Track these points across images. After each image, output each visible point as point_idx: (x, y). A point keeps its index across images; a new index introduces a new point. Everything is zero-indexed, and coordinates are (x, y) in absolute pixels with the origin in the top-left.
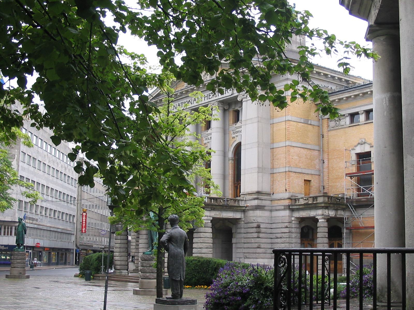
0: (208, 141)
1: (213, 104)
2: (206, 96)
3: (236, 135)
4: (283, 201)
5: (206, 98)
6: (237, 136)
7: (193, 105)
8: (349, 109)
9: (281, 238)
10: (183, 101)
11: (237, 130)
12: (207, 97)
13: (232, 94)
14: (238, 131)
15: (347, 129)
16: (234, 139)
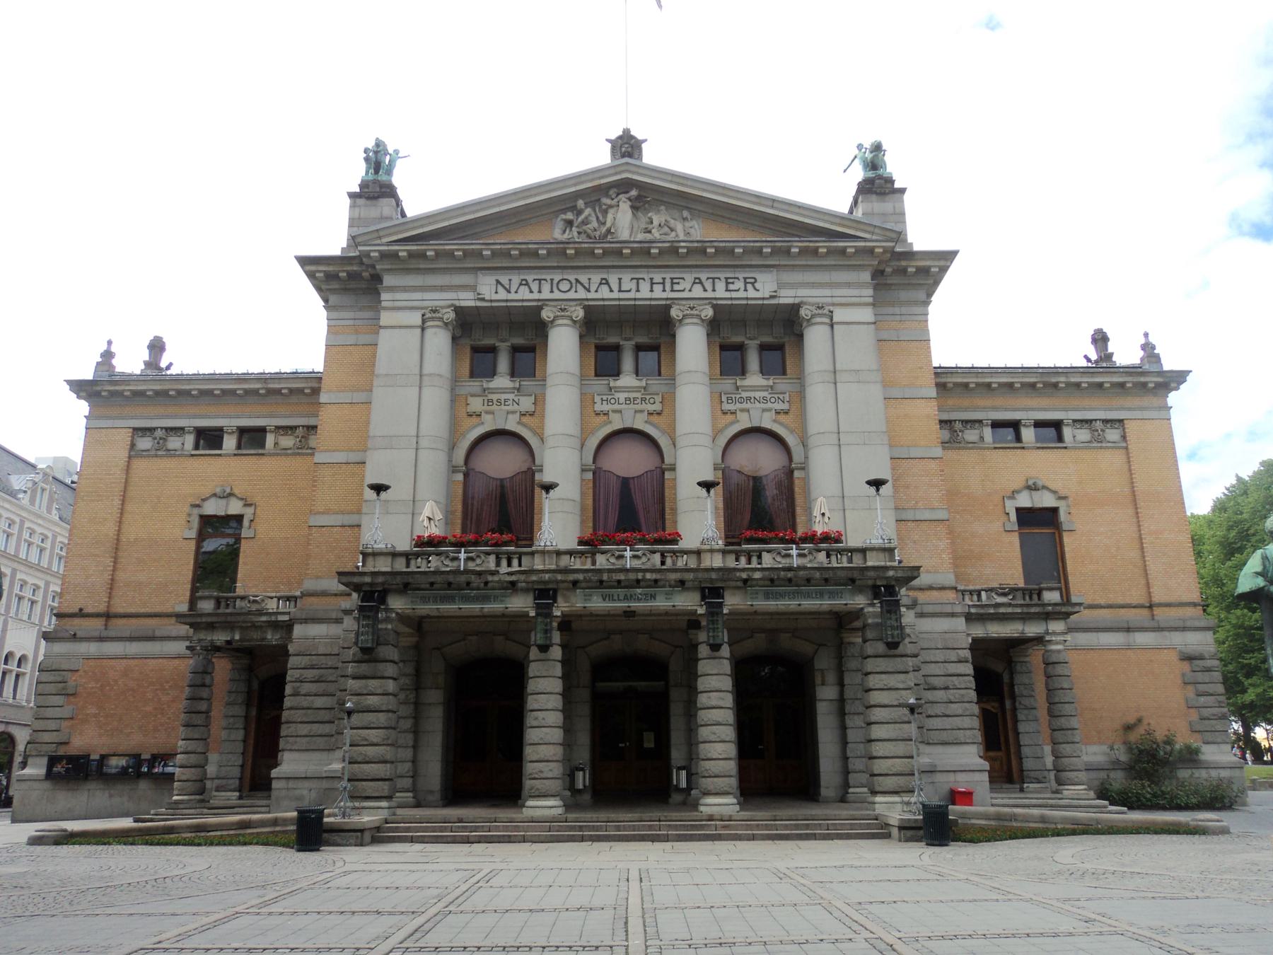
0: (616, 407)
1: (692, 308)
2: (658, 278)
3: (738, 406)
4: (935, 593)
5: (658, 288)
6: (742, 410)
7: (590, 296)
8: (995, 409)
9: (947, 688)
10: (548, 277)
11: (744, 395)
12: (663, 283)
13: (772, 297)
14: (749, 399)
15: (987, 452)
16: (730, 418)
